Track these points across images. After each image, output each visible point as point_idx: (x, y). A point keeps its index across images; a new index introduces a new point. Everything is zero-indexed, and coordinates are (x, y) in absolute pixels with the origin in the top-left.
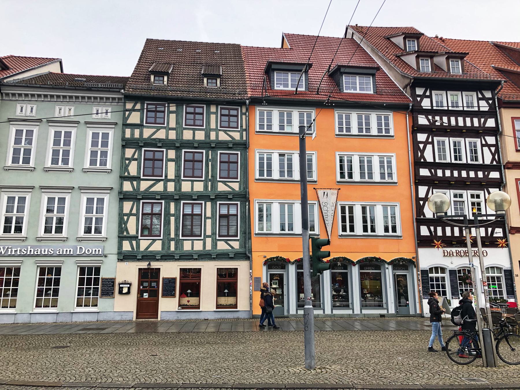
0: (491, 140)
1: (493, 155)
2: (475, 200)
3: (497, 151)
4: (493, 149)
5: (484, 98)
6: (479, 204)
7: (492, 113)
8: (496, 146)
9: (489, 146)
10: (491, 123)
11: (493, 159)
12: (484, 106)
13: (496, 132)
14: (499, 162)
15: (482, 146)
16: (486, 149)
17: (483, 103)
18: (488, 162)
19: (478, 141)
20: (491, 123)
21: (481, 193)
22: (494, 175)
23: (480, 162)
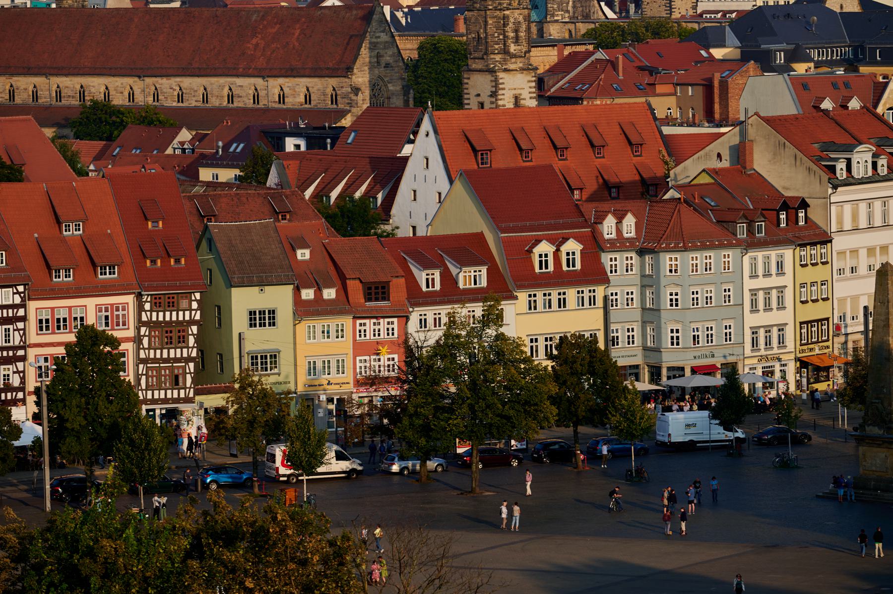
0: (20, 325)
1: (21, 337)
2: (6, 373)
3: (24, 334)
4: (21, 332)
5: (18, 293)
6: (8, 375)
7: (23, 305)
8: (24, 330)
9: (18, 330)
10: (21, 312)
11: (21, 340)
12: (18, 300)
13: (24, 319)
14: (25, 343)
15: (14, 330)
16: (16, 333)
17: (17, 296)
18: (17, 343)
19: (11, 327)
20: (21, 312)
21: (10, 367)
22: (21, 353)
23: (11, 344)
